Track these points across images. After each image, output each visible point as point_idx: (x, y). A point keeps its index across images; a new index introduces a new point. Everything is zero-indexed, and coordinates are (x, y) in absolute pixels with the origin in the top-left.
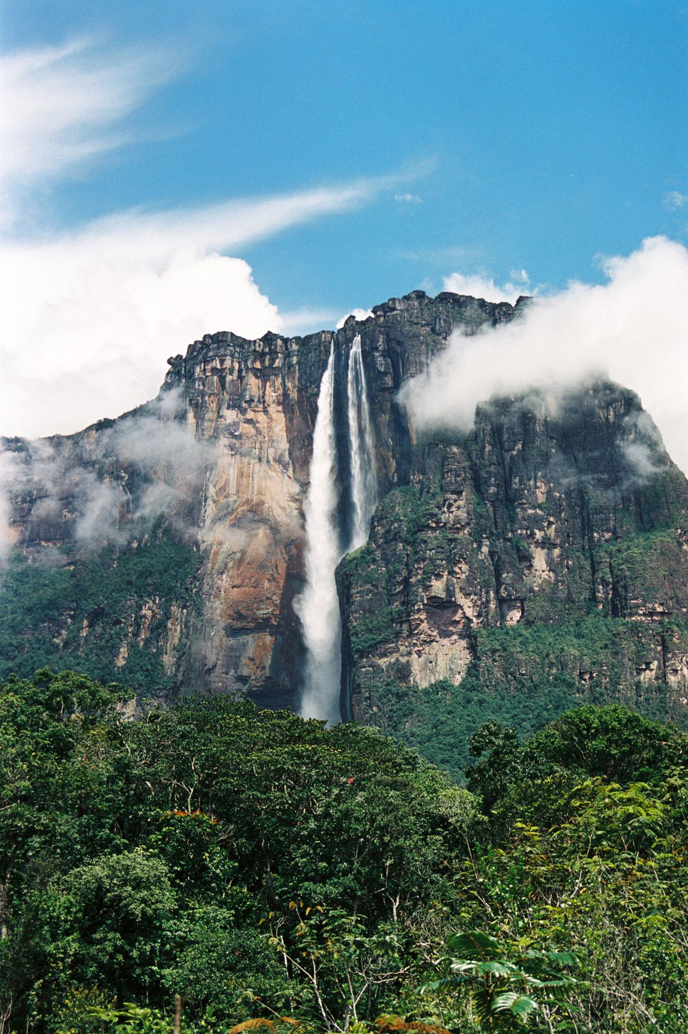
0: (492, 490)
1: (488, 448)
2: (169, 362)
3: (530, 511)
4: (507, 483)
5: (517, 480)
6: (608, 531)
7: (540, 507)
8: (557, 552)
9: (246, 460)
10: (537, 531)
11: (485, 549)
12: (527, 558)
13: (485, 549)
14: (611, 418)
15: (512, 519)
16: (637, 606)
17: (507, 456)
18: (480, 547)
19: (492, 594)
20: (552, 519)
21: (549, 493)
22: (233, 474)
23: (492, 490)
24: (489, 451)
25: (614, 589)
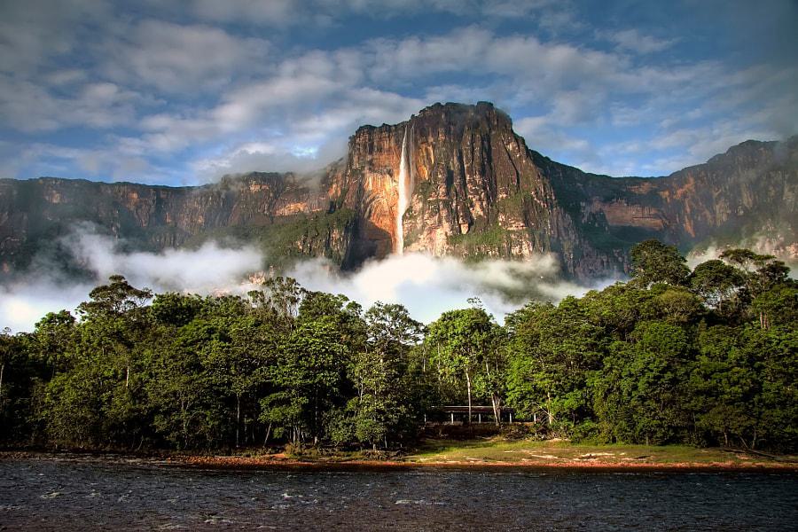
2: (350, 138)
11: (454, 204)
12: (472, 206)
13: (454, 204)
17: (465, 166)
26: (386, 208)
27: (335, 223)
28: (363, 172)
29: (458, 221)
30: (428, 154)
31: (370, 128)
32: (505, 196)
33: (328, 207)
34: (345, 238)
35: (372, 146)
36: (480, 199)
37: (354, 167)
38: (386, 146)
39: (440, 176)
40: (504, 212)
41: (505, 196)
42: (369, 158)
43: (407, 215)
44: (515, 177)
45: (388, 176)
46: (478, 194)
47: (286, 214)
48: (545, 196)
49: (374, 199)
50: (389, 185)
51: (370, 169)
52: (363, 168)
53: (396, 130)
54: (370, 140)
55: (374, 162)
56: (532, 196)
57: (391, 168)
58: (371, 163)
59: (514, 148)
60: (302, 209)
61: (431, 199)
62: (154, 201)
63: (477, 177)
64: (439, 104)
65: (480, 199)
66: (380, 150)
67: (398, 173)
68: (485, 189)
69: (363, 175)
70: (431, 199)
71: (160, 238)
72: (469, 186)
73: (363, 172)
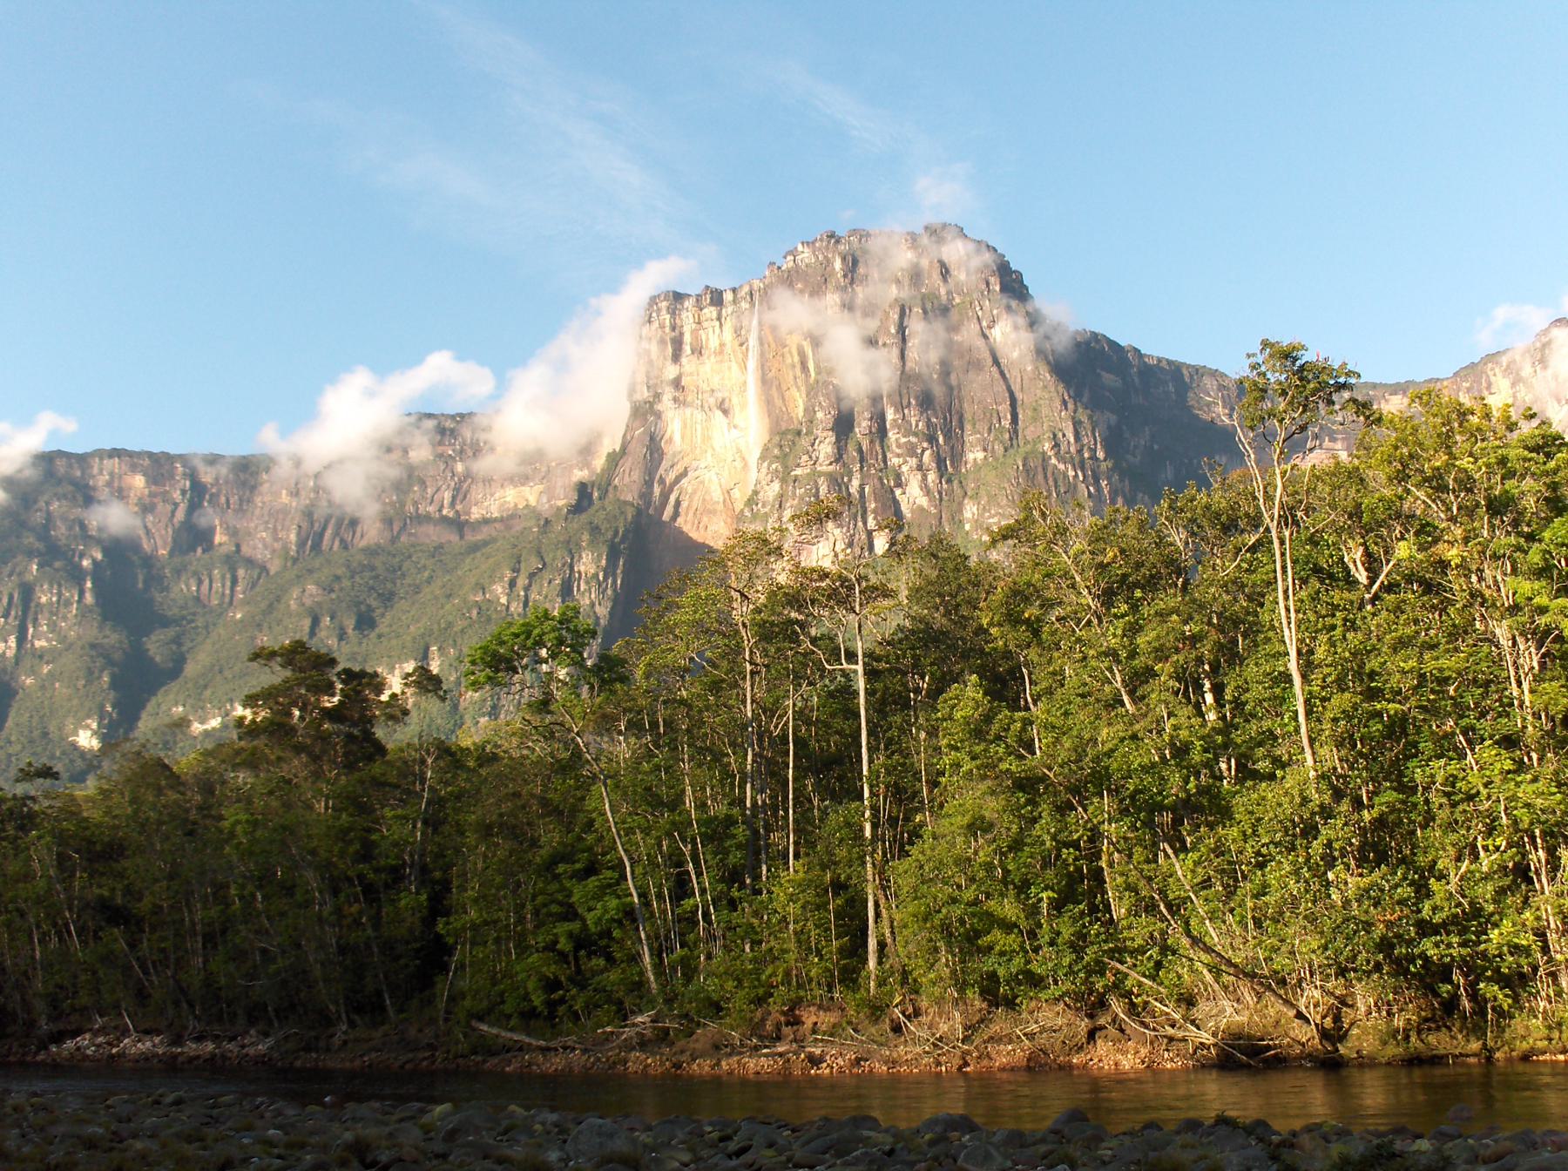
0: (865, 424)
3: (903, 440)
7: (916, 434)
9: (688, 411)
11: (855, 483)
12: (899, 485)
13: (855, 483)
19: (860, 524)
26: (717, 495)
27: (586, 537)
28: (658, 407)
29: (865, 523)
31: (678, 297)
33: (573, 498)
34: (609, 571)
35: (678, 344)
36: (920, 468)
38: (714, 343)
39: (820, 415)
40: (976, 497)
42: (671, 371)
43: (748, 514)
44: (1005, 408)
45: (719, 413)
47: (496, 515)
48: (1080, 452)
49: (684, 474)
51: (675, 400)
52: (657, 396)
53: (735, 301)
54: (673, 328)
56: (1044, 453)
57: (726, 394)
58: (677, 383)
60: (533, 502)
61: (798, 472)
62: (184, 492)
63: (913, 416)
64: (832, 236)
65: (920, 468)
66: (698, 351)
67: (744, 406)
68: (932, 439)
69: (658, 415)
70: (798, 472)
71: (200, 582)
72: (892, 435)
73: (658, 407)
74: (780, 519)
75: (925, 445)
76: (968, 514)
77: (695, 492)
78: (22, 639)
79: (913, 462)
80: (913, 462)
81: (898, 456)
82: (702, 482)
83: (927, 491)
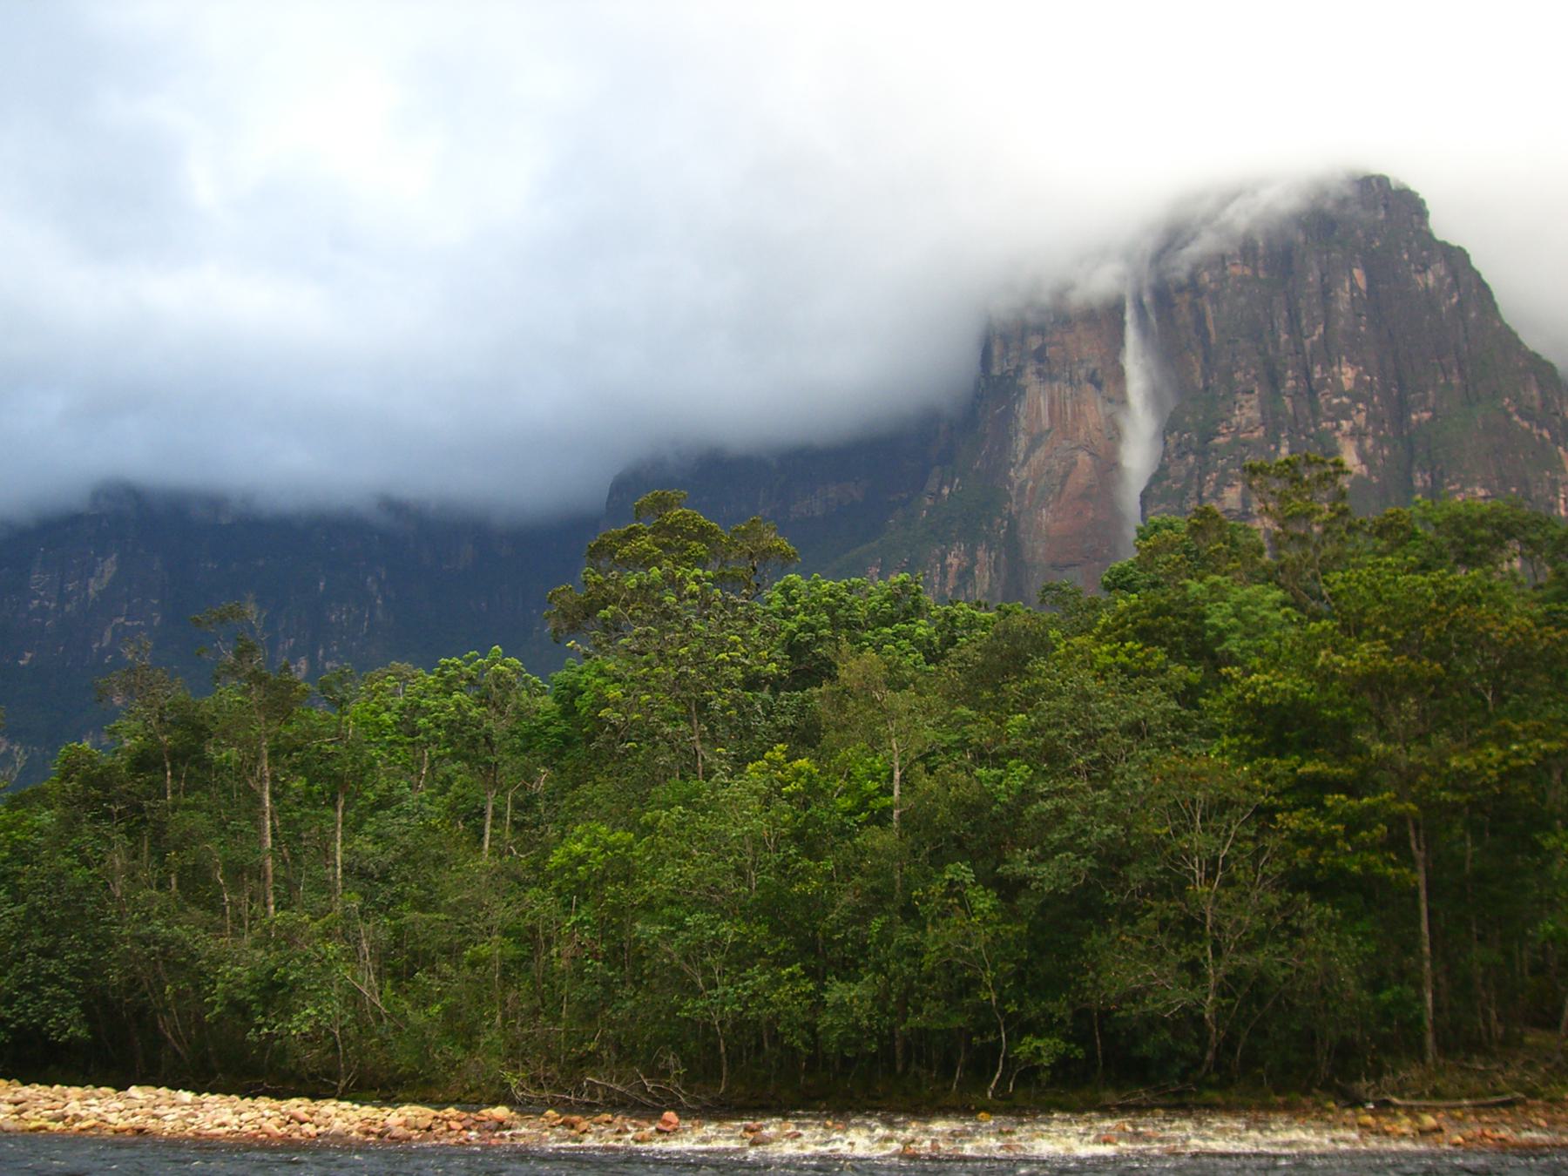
0: (1290, 384)
1: (1284, 337)
3: (1335, 401)
4: (1308, 375)
5: (1318, 368)
6: (1426, 410)
8: (1369, 442)
9: (1056, 386)
10: (1343, 422)
14: (1431, 281)
15: (1315, 413)
16: (1456, 492)
17: (1307, 343)
18: (1278, 449)
20: (1361, 406)
21: (1358, 380)
22: (1044, 403)
23: (1290, 384)
24: (1287, 342)
25: (1432, 476)
28: (1022, 381)
30: (1200, 319)
32: (1426, 415)
37: (996, 371)
41: (1426, 415)
45: (1089, 388)
46: (1349, 418)
50: (1094, 410)
51: (1039, 373)
52: (1019, 370)
55: (1049, 352)
58: (1040, 355)
59: (1440, 280)
68: (1368, 402)
69: (1022, 390)
70: (1220, 440)
73: (1022, 381)
74: (1199, 495)
75: (1361, 406)
76: (1419, 483)
77: (1066, 475)
78: (312, 661)
79: (1346, 425)
80: (1346, 425)
81: (1331, 419)
82: (1075, 464)
83: (1363, 457)
